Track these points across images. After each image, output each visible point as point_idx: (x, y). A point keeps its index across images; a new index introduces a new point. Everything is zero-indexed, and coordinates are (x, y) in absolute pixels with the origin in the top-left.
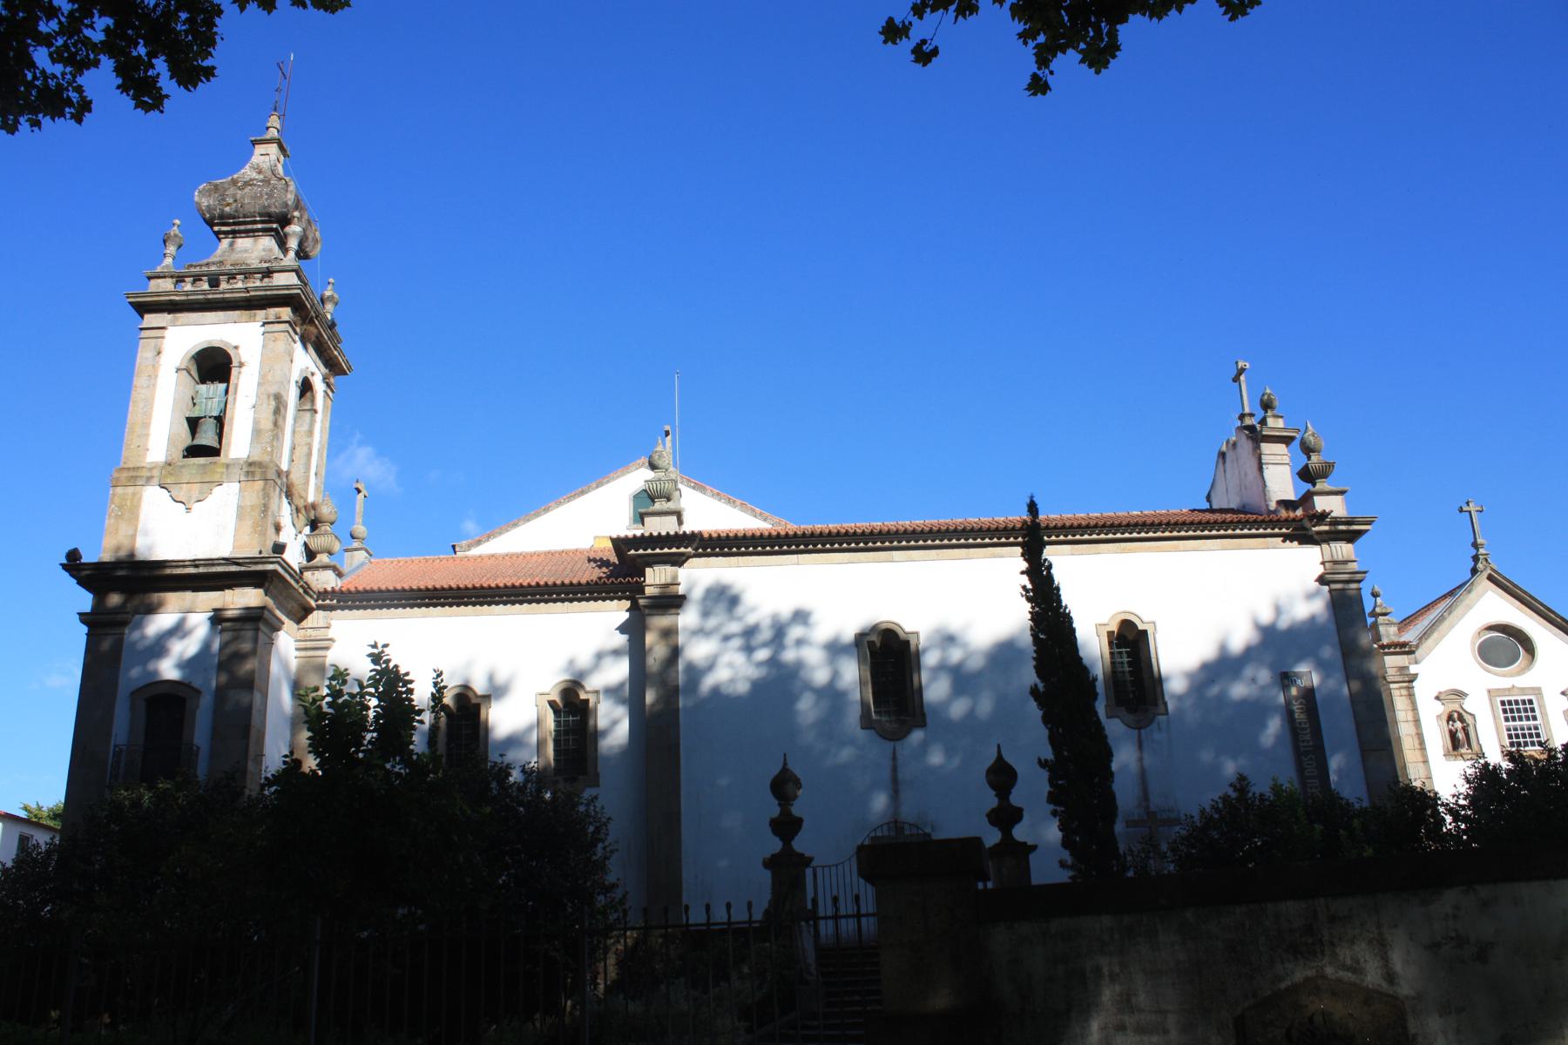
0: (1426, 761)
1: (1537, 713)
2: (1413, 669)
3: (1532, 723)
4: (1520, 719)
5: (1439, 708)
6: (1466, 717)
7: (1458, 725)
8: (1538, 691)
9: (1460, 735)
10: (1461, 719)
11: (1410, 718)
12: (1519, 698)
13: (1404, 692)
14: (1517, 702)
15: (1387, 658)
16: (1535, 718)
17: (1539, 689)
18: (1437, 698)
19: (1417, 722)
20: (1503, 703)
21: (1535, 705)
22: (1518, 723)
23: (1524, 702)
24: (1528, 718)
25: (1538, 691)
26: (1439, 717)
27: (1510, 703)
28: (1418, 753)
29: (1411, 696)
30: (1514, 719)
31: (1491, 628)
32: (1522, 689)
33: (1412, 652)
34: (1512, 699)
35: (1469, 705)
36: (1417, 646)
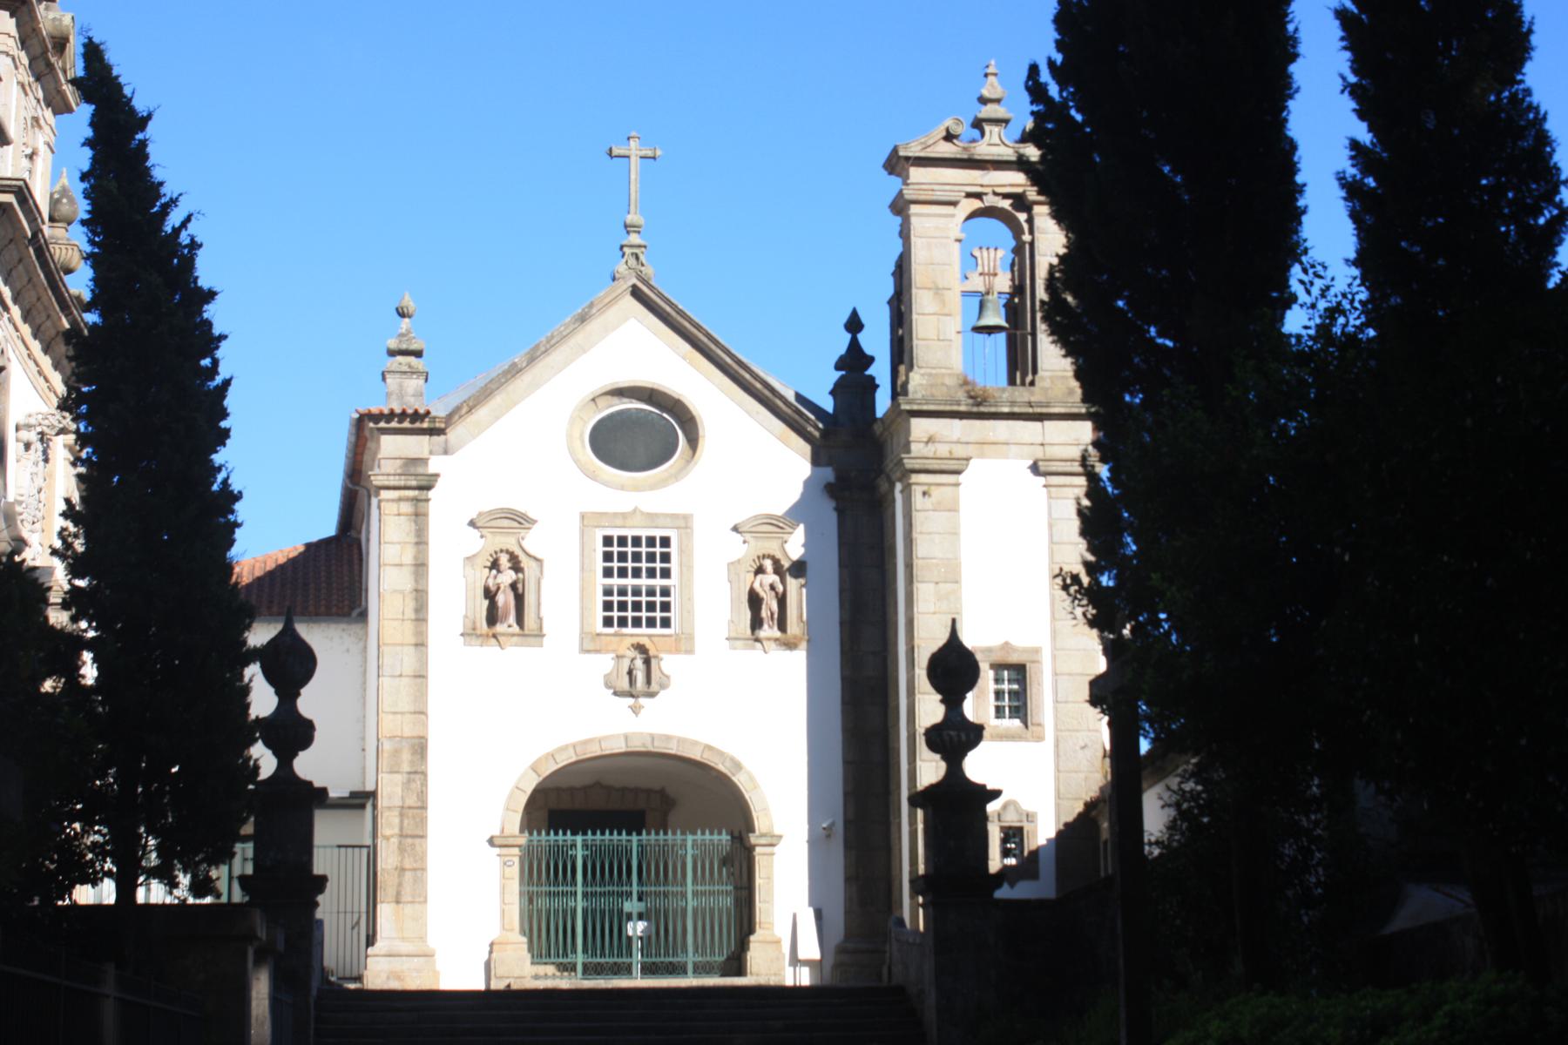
0: (421, 645)
1: (674, 566)
2: (435, 464)
3: (658, 582)
4: (637, 573)
5: (474, 543)
6: (525, 562)
7: (508, 576)
8: (684, 522)
9: (505, 599)
10: (516, 567)
11: (408, 557)
12: (644, 533)
13: (406, 508)
14: (637, 541)
15: (386, 440)
16: (666, 573)
17: (687, 518)
18: (472, 524)
19: (420, 567)
20: (608, 541)
21: (673, 550)
22: (630, 582)
23: (651, 541)
24: (651, 573)
25: (684, 522)
26: (469, 559)
27: (622, 541)
28: (409, 627)
29: (419, 517)
30: (623, 573)
31: (620, 392)
32: (652, 518)
33: (439, 432)
34: (629, 533)
35: (533, 542)
36: (449, 419)
